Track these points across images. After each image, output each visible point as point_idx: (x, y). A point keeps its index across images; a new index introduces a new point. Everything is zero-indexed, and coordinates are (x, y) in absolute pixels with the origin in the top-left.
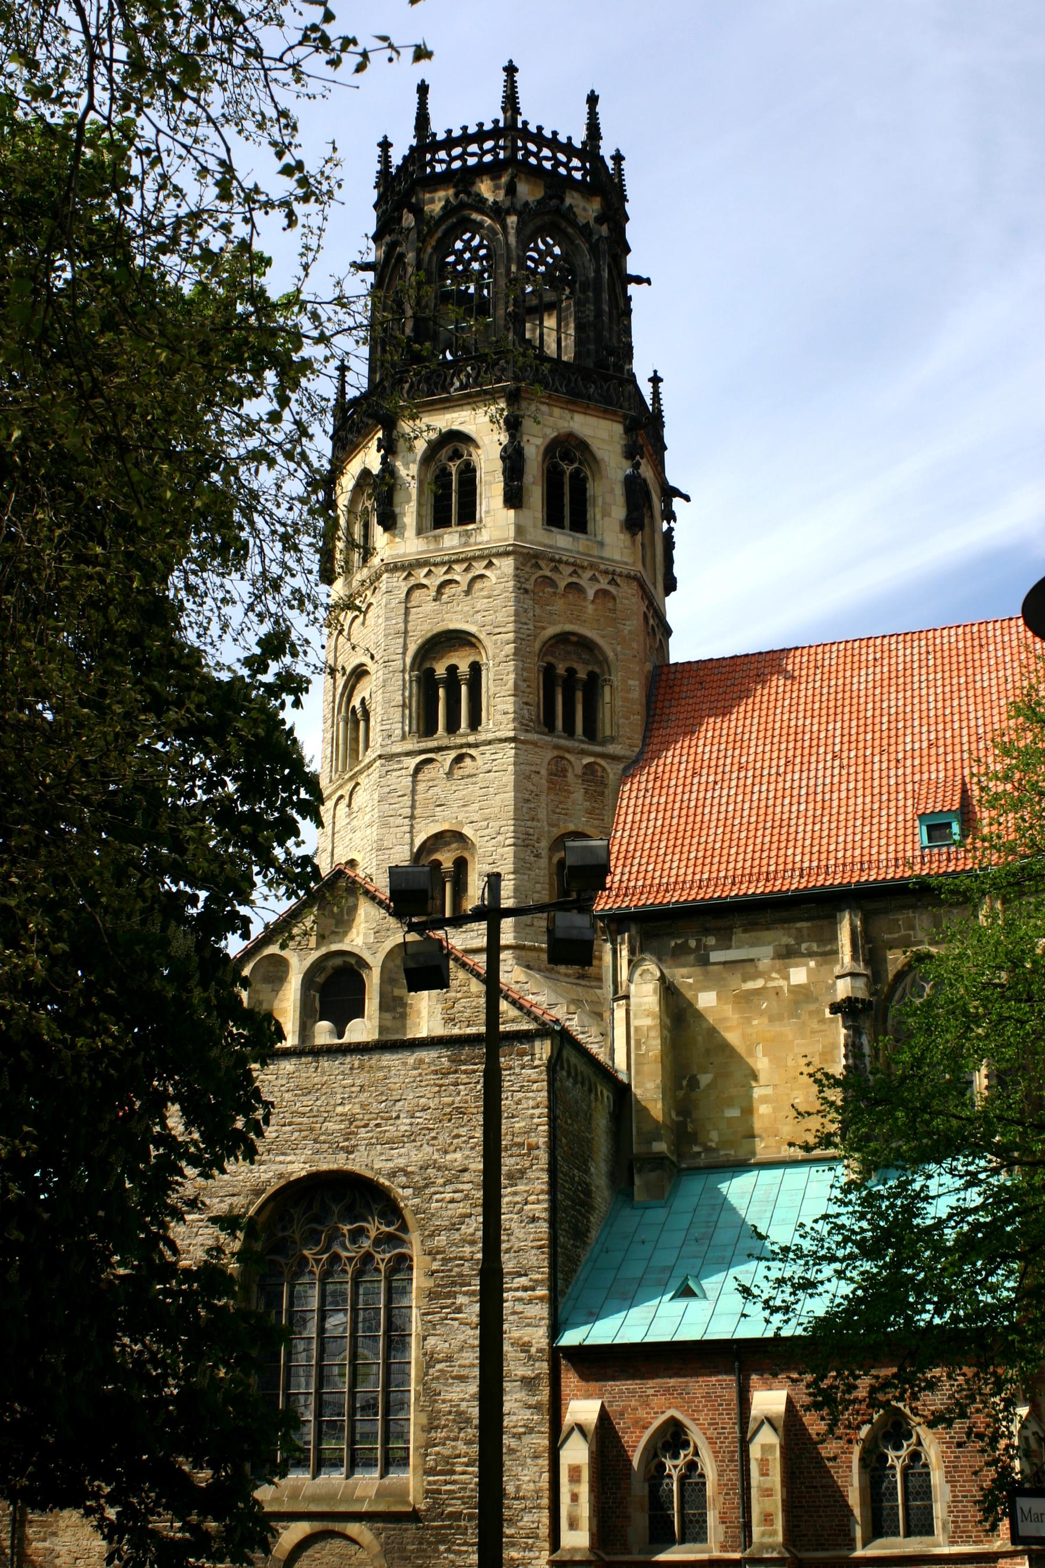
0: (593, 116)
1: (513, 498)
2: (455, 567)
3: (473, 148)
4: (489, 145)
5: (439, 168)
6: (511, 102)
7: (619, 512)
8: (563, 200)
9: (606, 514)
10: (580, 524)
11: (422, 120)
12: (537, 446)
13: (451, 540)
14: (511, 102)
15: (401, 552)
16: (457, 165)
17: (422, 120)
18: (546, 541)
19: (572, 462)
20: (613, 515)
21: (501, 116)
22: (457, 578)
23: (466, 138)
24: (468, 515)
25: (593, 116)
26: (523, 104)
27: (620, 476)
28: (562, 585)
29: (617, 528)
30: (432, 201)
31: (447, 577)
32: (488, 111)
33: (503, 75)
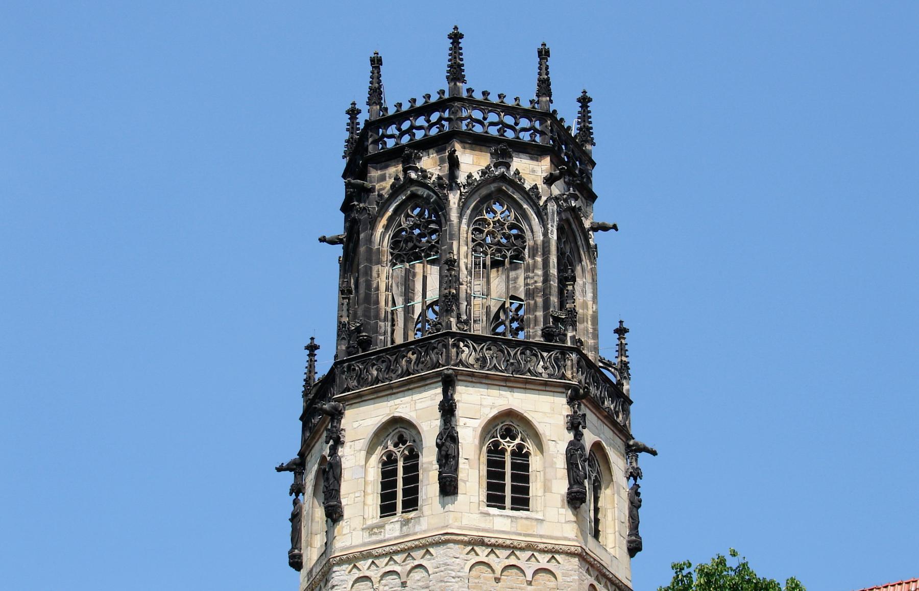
0: (543, 68)
1: (449, 487)
2: (395, 557)
3: (421, 121)
4: (434, 117)
5: (391, 143)
6: (456, 73)
7: (562, 486)
8: (508, 166)
9: (547, 489)
10: (522, 502)
11: (376, 94)
12: (474, 429)
13: (393, 529)
14: (456, 73)
15: (348, 544)
16: (406, 139)
17: (376, 94)
18: (483, 525)
19: (513, 438)
20: (554, 489)
21: (446, 86)
22: (397, 568)
23: (415, 112)
24: (411, 503)
25: (543, 68)
26: (467, 72)
27: (563, 447)
28: (498, 568)
29: (559, 504)
30: (383, 178)
31: (388, 569)
32: (433, 83)
33: (448, 43)
